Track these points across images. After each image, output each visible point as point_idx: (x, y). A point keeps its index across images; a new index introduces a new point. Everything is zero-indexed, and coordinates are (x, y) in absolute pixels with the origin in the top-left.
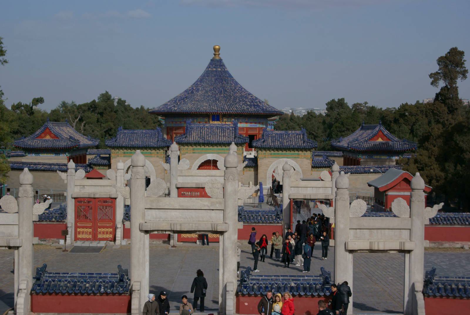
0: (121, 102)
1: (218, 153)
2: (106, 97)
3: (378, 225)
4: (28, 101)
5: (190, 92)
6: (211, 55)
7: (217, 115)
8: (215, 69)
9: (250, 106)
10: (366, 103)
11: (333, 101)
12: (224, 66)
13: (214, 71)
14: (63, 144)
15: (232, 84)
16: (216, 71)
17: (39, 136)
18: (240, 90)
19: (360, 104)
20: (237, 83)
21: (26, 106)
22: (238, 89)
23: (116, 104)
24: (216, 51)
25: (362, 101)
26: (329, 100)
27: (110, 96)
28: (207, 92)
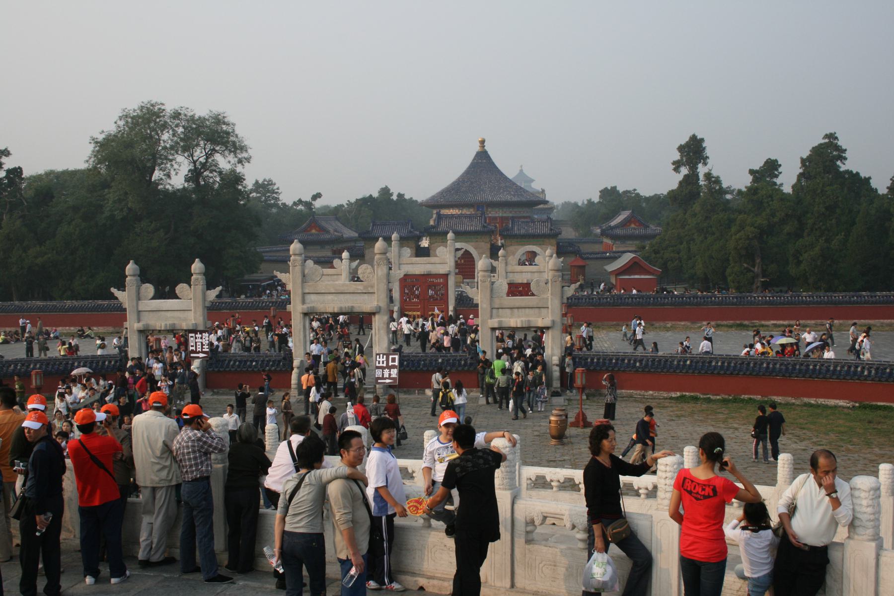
0: (400, 196)
1: (466, 242)
2: (385, 192)
3: (517, 305)
4: (307, 198)
6: (477, 148)
9: (514, 195)
10: (635, 190)
11: (606, 188)
12: (489, 157)
14: (327, 236)
17: (305, 230)
19: (629, 192)
20: (502, 174)
21: (306, 202)
23: (395, 197)
24: (483, 142)
25: (630, 189)
26: (602, 188)
27: (389, 190)
28: (472, 183)
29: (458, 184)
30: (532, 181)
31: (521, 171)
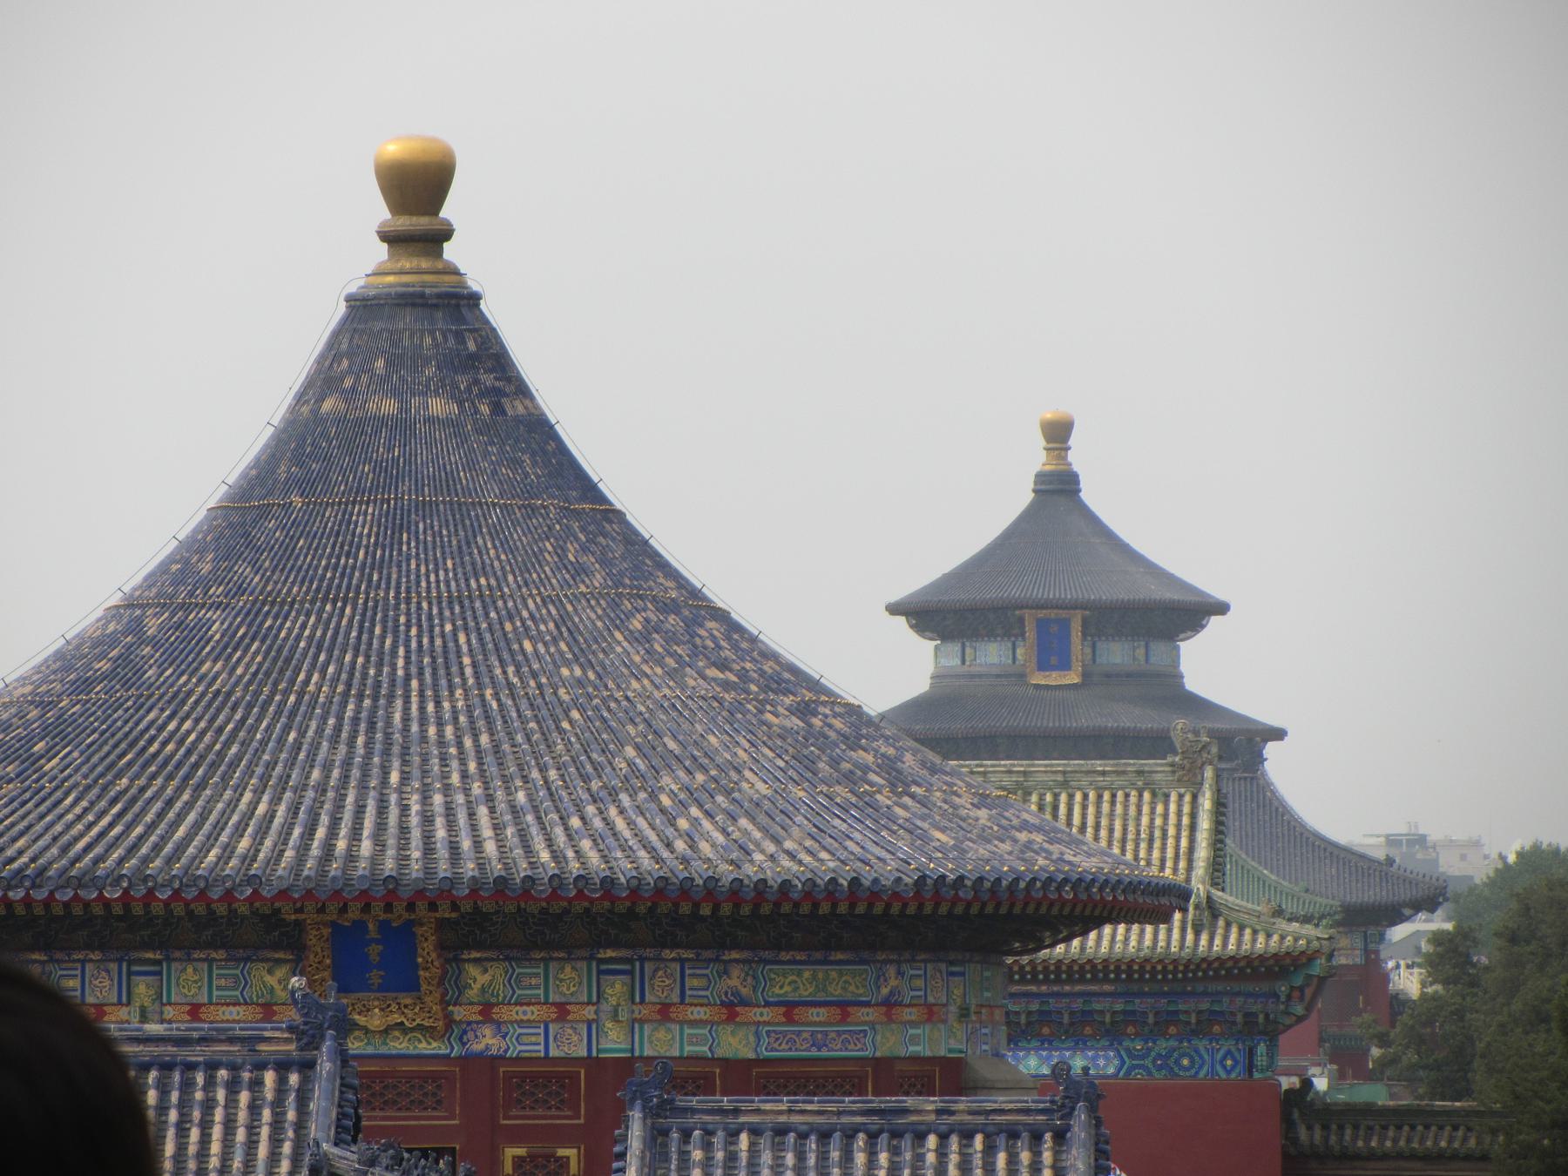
5: (104, 666)
6: (352, 250)
7: (384, 926)
8: (389, 407)
9: (772, 816)
13: (382, 421)
15: (580, 571)
16: (402, 427)
18: (670, 638)
22: (651, 628)
24: (418, 189)
29: (126, 670)
30: (1192, 612)
31: (1058, 488)
